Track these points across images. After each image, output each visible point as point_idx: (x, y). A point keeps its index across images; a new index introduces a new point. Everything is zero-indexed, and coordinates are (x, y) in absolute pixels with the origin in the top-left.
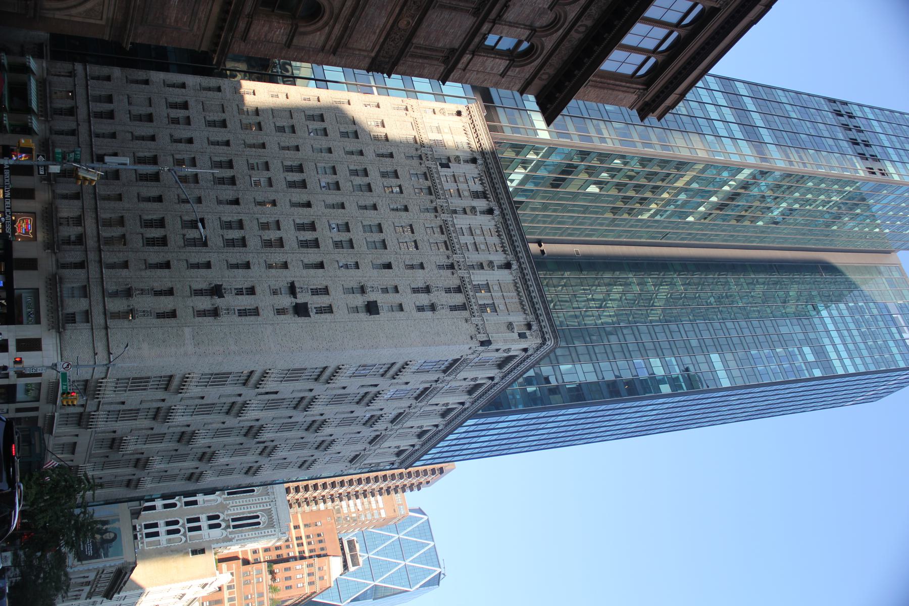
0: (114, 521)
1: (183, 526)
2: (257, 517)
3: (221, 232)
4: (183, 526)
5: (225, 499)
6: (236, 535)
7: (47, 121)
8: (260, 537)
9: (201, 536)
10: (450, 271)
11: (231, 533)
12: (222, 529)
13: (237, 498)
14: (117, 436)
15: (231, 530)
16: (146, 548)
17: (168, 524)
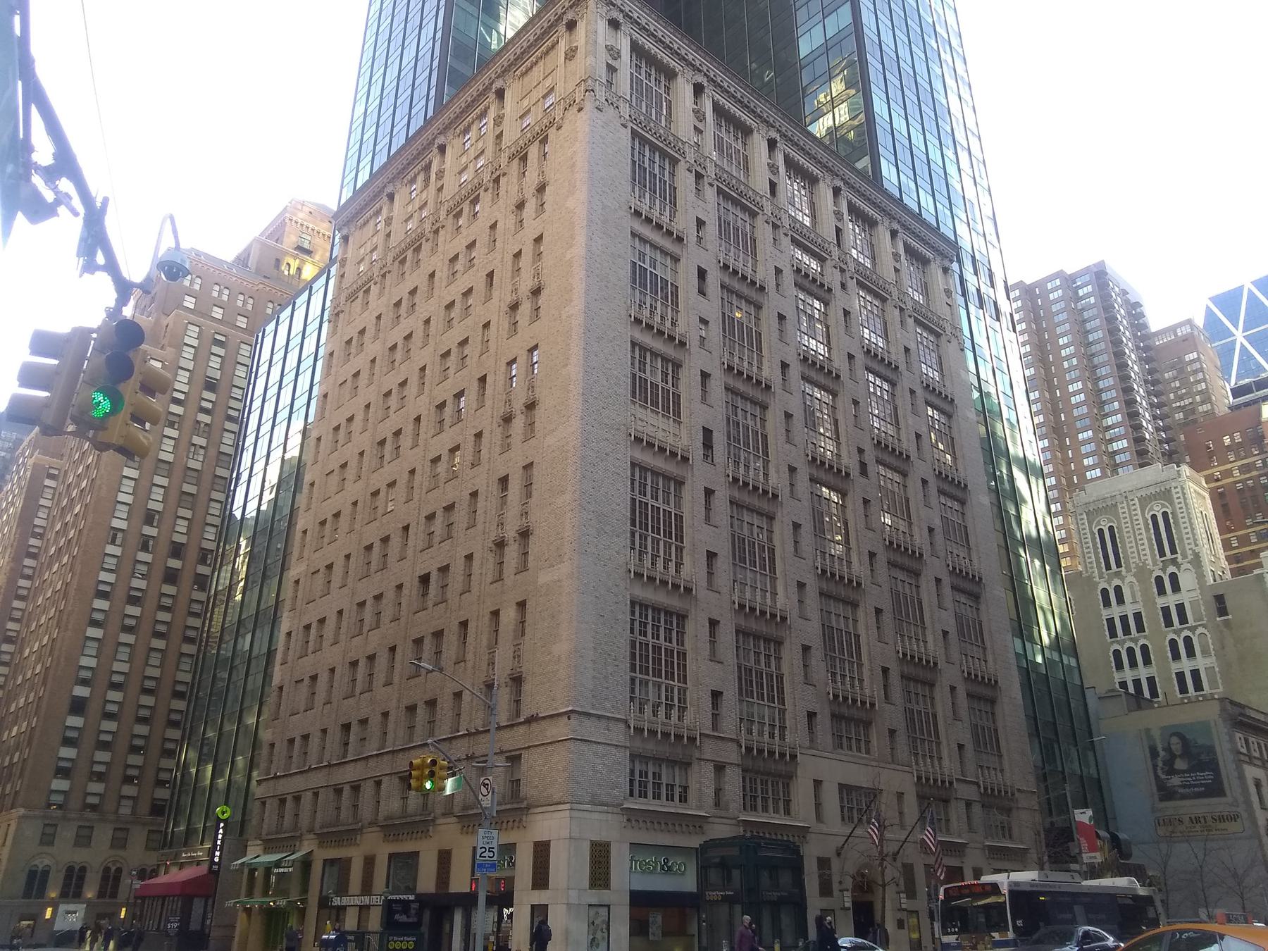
1: (1178, 632)
2: (1154, 517)
3: (436, 546)
4: (1178, 632)
5: (1128, 570)
6: (1188, 547)
7: (300, 838)
8: (1187, 509)
10: (503, 180)
11: (1185, 557)
13: (1125, 552)
14: (827, 712)
15: (1179, 556)
16: (1221, 689)
17: (1176, 656)
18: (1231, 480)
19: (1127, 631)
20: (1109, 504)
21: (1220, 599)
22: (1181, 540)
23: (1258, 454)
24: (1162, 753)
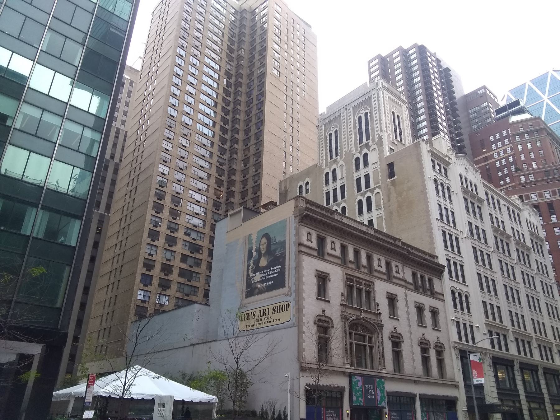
0: (250, 242)
1: (363, 195)
2: (360, 118)
4: (363, 195)
5: (341, 157)
6: (376, 133)
11: (373, 140)
12: (369, 151)
13: (341, 146)
18: (493, 160)
19: (335, 200)
20: (337, 116)
21: (391, 166)
22: (373, 129)
23: (508, 144)
24: (254, 254)
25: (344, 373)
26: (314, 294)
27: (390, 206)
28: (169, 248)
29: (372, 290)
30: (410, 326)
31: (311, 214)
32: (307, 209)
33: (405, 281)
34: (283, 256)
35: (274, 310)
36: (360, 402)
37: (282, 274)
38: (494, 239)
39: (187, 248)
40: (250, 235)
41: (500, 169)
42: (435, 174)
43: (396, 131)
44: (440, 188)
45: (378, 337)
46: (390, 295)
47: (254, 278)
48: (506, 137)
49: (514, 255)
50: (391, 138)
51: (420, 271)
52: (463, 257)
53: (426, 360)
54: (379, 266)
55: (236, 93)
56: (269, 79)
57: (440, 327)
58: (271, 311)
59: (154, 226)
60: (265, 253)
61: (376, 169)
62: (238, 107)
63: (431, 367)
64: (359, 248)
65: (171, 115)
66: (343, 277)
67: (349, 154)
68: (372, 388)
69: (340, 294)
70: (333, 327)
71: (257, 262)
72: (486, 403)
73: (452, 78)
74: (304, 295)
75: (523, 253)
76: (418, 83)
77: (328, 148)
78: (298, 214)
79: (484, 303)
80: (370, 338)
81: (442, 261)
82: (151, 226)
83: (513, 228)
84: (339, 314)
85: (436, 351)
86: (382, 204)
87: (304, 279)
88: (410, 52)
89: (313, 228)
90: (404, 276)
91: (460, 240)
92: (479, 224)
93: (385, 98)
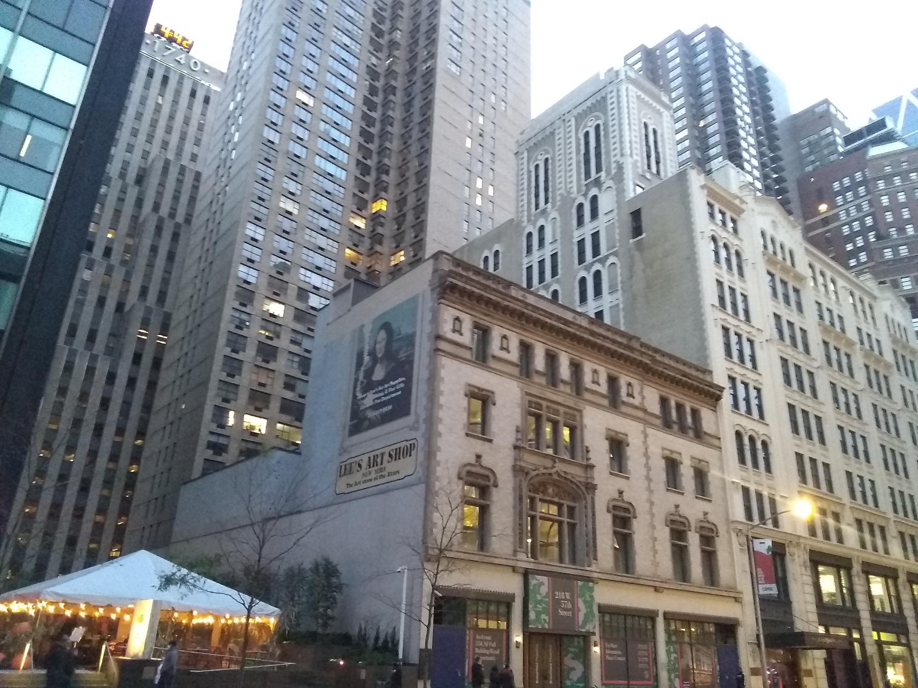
0: (361, 340)
1: (587, 269)
2: (587, 135)
6: (613, 159)
9: (610, 229)
11: (608, 172)
13: (554, 186)
19: (542, 279)
21: (636, 215)
22: (608, 153)
23: (864, 196)
24: (367, 358)
25: (514, 569)
26: (462, 426)
27: (632, 286)
28: (264, 365)
29: (577, 424)
30: (651, 491)
31: (460, 284)
32: (451, 273)
33: (645, 411)
34: (409, 361)
35: (390, 455)
36: (542, 621)
37: (407, 391)
38: (822, 346)
39: (295, 365)
40: (363, 326)
41: (851, 238)
42: (714, 227)
43: (649, 157)
44: (723, 254)
45: (586, 508)
46: (613, 434)
47: (365, 401)
48: (860, 184)
49: (860, 375)
50: (638, 167)
51: (677, 395)
52: (760, 374)
53: (680, 554)
54: (594, 382)
55: (386, 104)
56: (440, 79)
57: (710, 496)
58: (386, 457)
59: (238, 327)
60: (382, 357)
61: (612, 221)
62: (389, 128)
63: (690, 565)
64: (555, 350)
65: (269, 141)
66: (522, 398)
67: (567, 199)
68: (568, 597)
69: (514, 428)
70: (496, 486)
71: (369, 372)
72: (797, 631)
73: (770, 84)
74: (441, 428)
75: (877, 372)
76: (709, 91)
77: (533, 190)
78: (437, 285)
79: (799, 456)
80: (571, 510)
81: (720, 378)
82: (232, 328)
83: (859, 330)
84: (509, 462)
85: (702, 536)
86: (619, 282)
87: (442, 400)
88: (696, 40)
89: (468, 311)
90: (642, 403)
91: (757, 346)
92: (795, 318)
93: (631, 99)
